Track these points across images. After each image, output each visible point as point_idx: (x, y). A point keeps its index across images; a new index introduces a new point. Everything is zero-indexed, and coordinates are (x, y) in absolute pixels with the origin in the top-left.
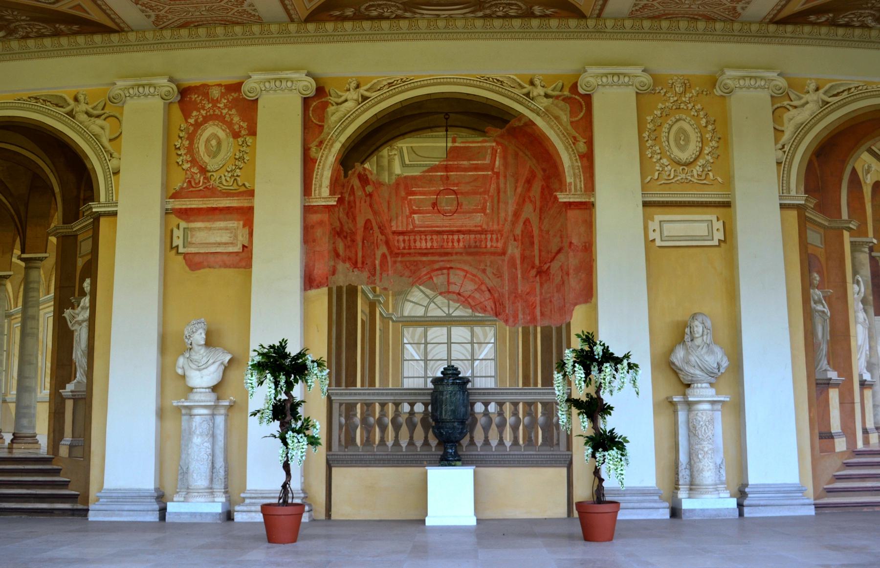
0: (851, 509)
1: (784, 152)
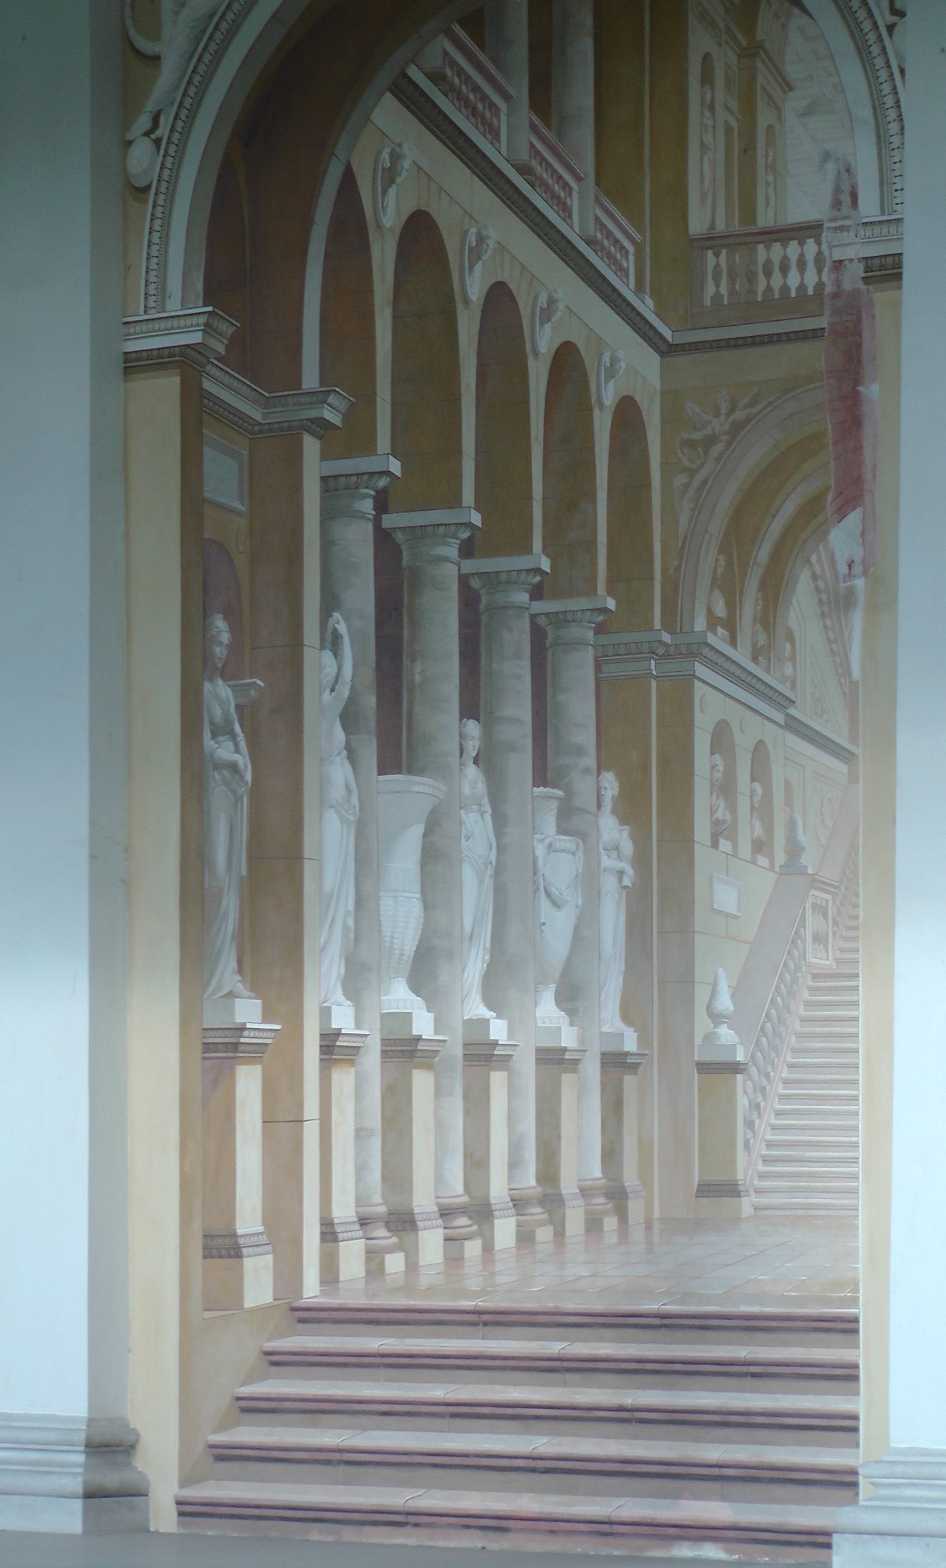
0: (275, 1530)
1: (158, 142)
